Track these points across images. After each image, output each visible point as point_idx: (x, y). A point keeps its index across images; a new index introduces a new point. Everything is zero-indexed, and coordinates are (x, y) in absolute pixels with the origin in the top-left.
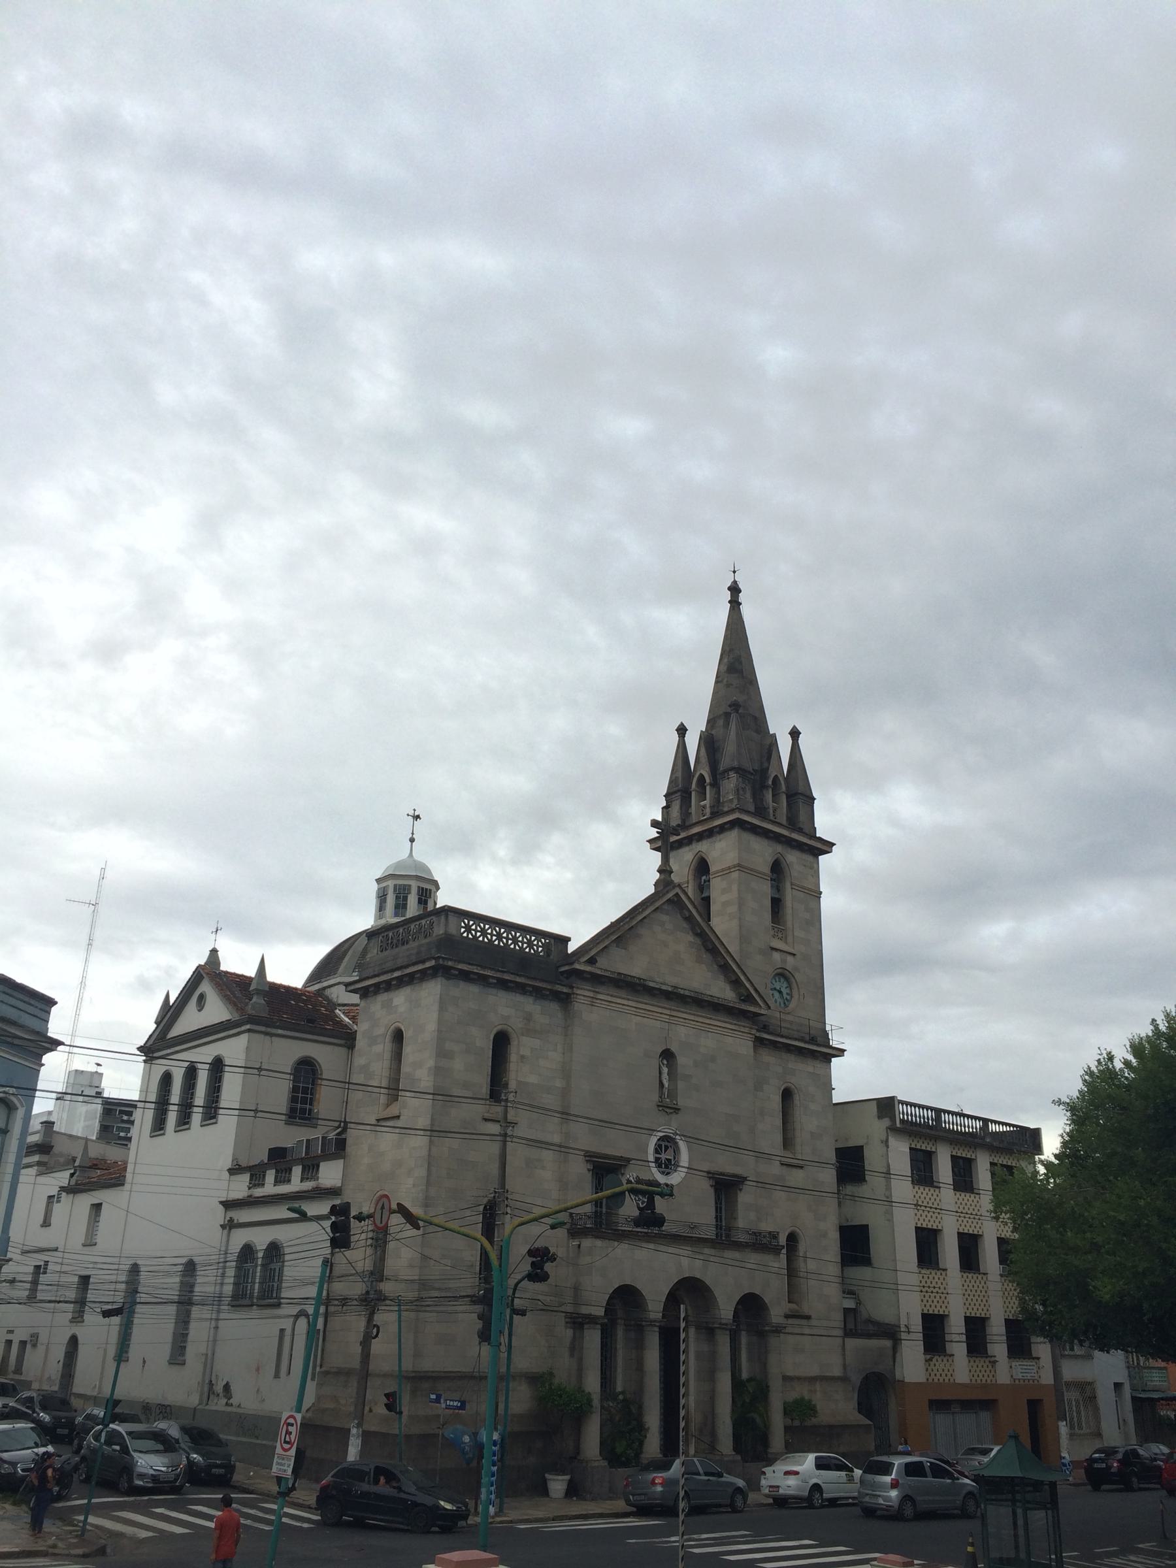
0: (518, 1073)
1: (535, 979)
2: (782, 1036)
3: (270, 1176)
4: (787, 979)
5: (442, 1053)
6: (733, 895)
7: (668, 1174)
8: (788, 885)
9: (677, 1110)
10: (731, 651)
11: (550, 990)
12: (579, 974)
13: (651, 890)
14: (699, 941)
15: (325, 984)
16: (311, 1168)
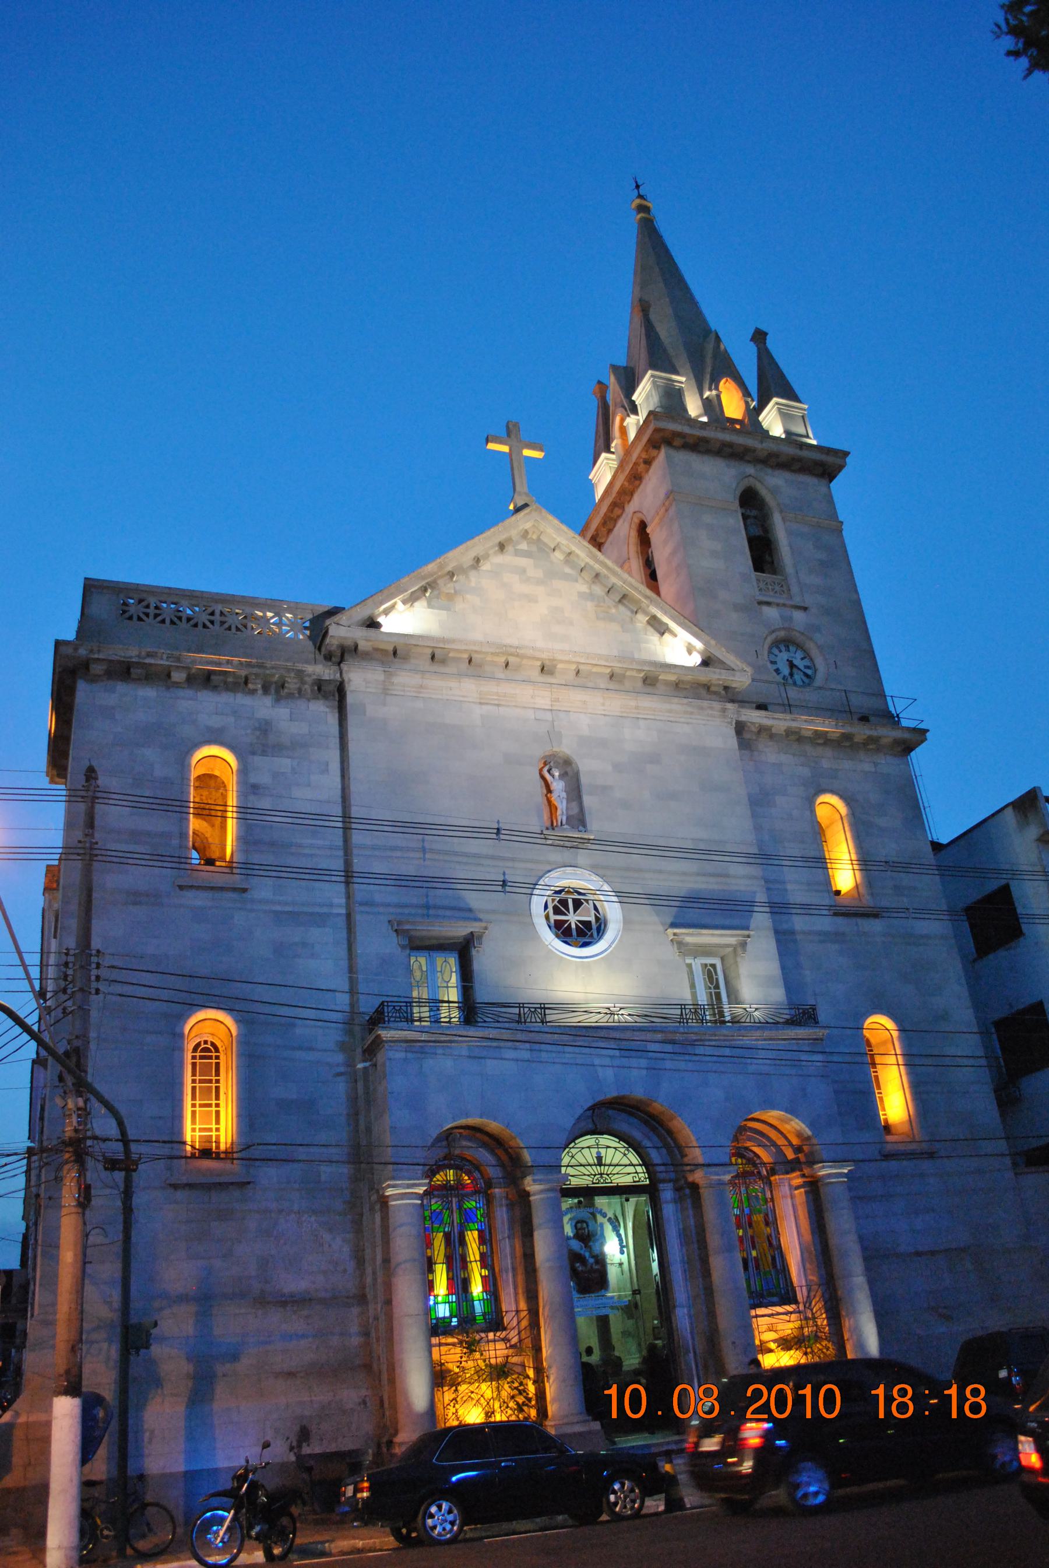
8: (777, 519)
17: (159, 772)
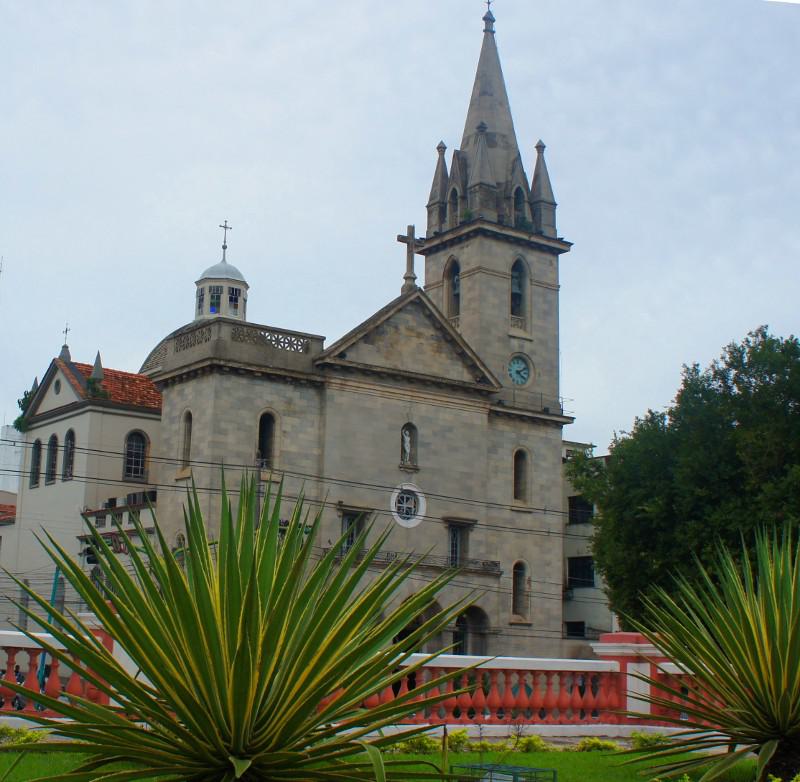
0: (281, 444)
3: (109, 518)
4: (524, 361)
5: (218, 431)
7: (408, 519)
8: (528, 282)
9: (416, 470)
11: (307, 380)
12: (330, 366)
13: (399, 294)
14: (439, 334)
17: (248, 423)
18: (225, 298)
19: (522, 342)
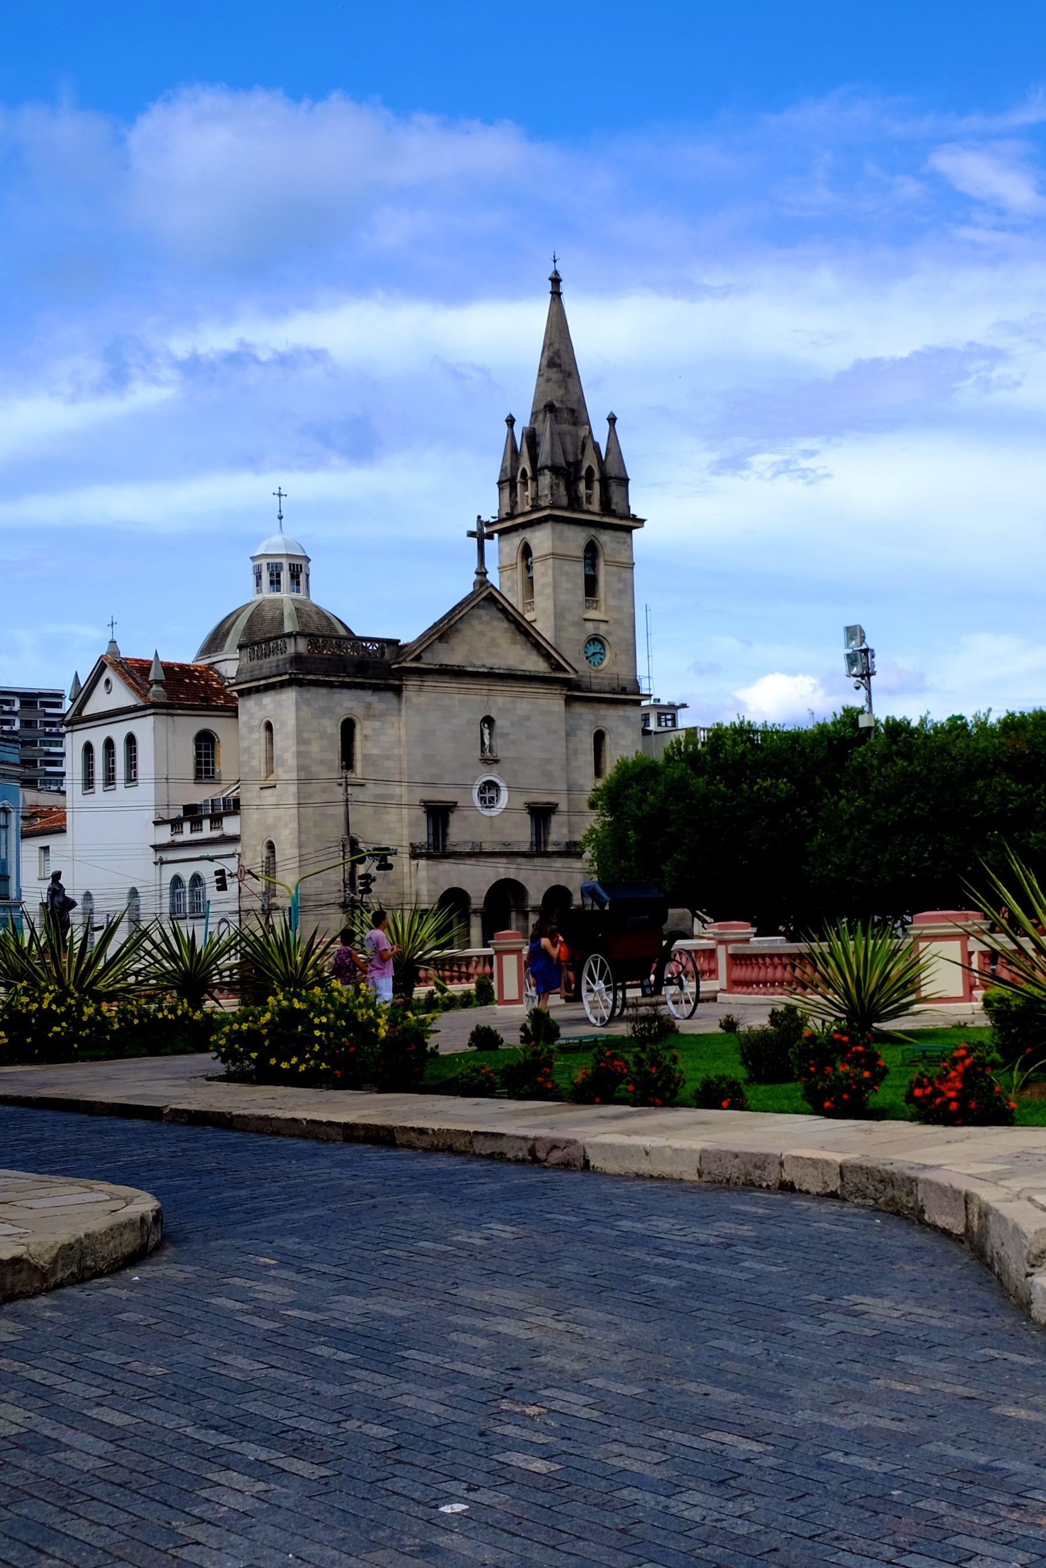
1: (371, 678)
2: (592, 692)
3: (187, 826)
4: (601, 642)
5: (301, 741)
6: (549, 579)
10: (551, 344)
13: (471, 589)
14: (513, 627)
15: (214, 659)
16: (216, 819)
17: (329, 731)
18: (285, 576)
19: (596, 624)
